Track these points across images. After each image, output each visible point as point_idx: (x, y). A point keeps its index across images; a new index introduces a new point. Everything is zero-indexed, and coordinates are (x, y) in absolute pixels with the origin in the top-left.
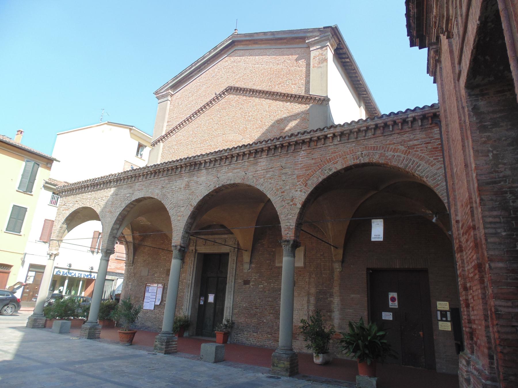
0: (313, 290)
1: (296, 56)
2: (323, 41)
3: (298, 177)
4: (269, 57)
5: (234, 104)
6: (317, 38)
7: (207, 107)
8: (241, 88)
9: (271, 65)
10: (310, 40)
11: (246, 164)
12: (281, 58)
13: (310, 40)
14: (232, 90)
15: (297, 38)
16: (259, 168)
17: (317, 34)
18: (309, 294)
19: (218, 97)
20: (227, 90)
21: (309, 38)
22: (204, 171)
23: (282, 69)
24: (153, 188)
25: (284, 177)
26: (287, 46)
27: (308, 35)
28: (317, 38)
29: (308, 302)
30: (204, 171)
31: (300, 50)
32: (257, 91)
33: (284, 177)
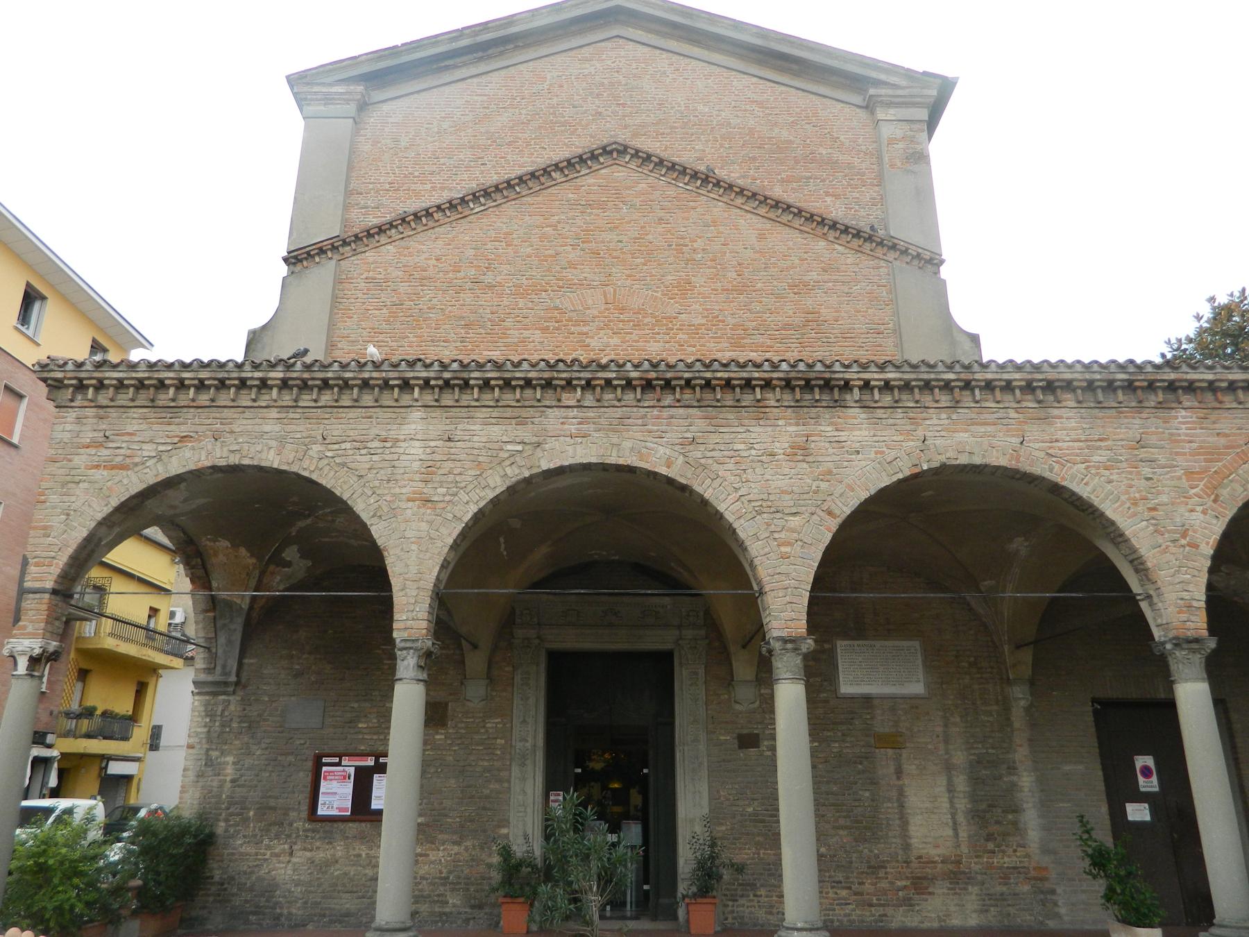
0: (960, 758)
3: (1189, 474)
11: (1013, 414)
16: (1061, 435)
18: (949, 768)
25: (1147, 471)
29: (951, 789)
33: (1147, 471)
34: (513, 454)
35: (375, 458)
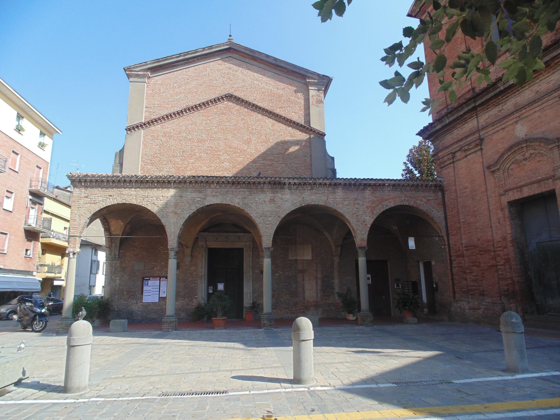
1: (295, 88)
2: (321, 85)
4: (269, 79)
5: (235, 113)
6: (316, 81)
7: (203, 106)
8: (243, 100)
9: (271, 88)
10: (310, 81)
12: (282, 85)
13: (310, 81)
14: (230, 97)
15: (296, 73)
17: (317, 78)
19: (216, 101)
20: (226, 96)
21: (309, 78)
22: (287, 190)
23: (283, 95)
24: (231, 196)
26: (285, 75)
27: (309, 75)
28: (316, 81)
30: (287, 190)
31: (298, 83)
32: (260, 108)
34: (198, 201)
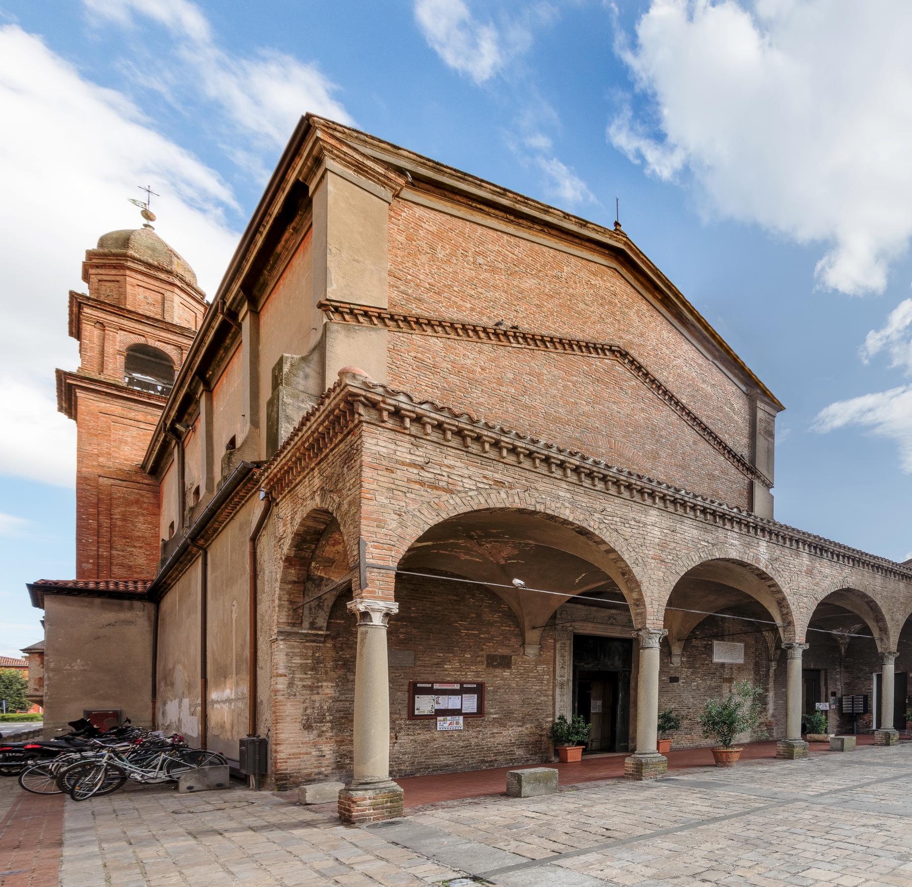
35: (634, 531)
